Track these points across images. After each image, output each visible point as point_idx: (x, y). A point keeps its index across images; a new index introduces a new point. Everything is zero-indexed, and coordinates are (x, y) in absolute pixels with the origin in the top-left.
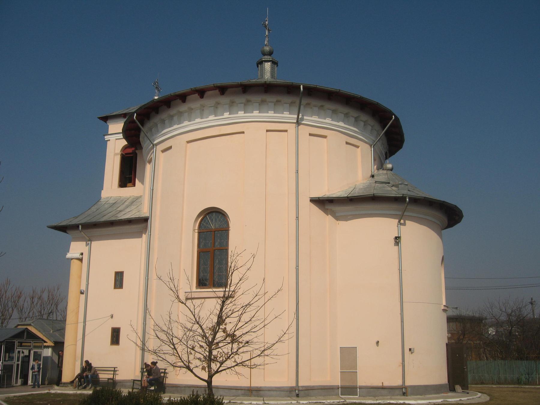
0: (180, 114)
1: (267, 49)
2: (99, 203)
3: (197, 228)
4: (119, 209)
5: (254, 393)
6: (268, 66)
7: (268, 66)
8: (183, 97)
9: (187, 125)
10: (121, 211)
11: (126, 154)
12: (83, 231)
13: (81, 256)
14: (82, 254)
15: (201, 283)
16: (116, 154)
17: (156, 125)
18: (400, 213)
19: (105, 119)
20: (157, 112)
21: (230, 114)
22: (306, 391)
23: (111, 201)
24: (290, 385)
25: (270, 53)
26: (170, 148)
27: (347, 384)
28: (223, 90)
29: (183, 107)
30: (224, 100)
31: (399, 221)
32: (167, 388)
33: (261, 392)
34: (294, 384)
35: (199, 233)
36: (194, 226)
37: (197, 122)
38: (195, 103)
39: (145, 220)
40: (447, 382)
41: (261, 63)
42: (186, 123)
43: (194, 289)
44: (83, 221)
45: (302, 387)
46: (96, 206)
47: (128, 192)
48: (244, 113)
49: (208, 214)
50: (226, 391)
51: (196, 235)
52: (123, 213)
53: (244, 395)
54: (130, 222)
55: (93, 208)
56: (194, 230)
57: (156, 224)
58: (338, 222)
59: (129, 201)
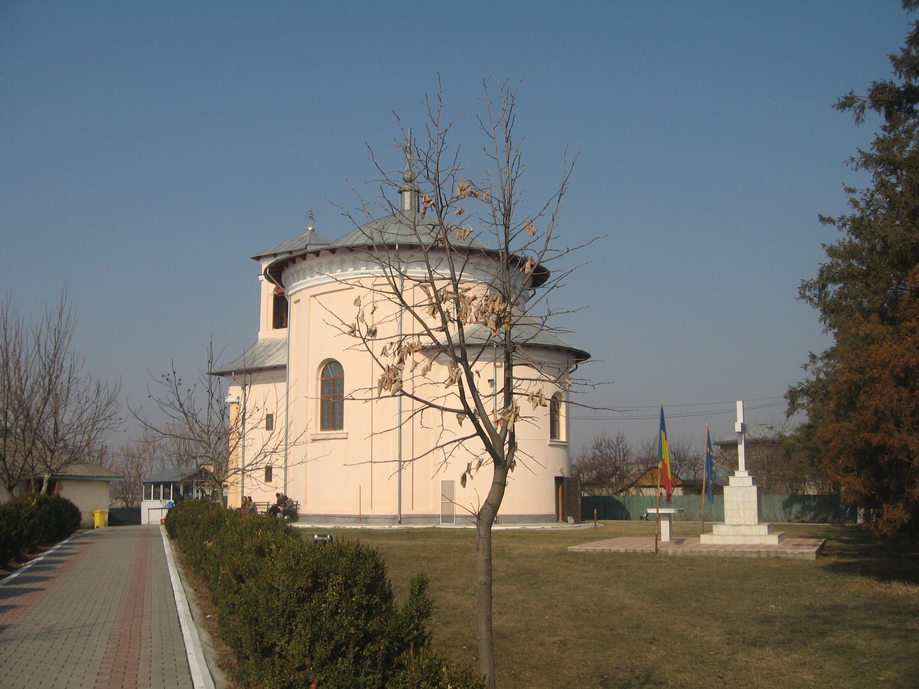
0: (304, 270)
1: (407, 176)
2: (256, 345)
3: (320, 376)
4: (270, 353)
5: (363, 520)
6: (407, 195)
7: (407, 195)
8: (304, 257)
9: (309, 281)
10: (270, 356)
11: (279, 294)
12: (236, 376)
13: (238, 400)
14: (238, 398)
15: (324, 426)
16: (269, 295)
17: (293, 275)
18: (492, 356)
19: (258, 258)
20: (287, 266)
21: (342, 271)
22: (408, 519)
23: (266, 344)
24: (393, 514)
25: (411, 181)
26: (298, 301)
27: (447, 513)
28: (333, 251)
29: (304, 264)
30: (336, 258)
31: (495, 365)
32: (300, 518)
33: (369, 520)
34: (396, 513)
35: (322, 381)
36: (317, 375)
37: (317, 279)
38: (312, 261)
39: (283, 367)
40: (554, 513)
41: (401, 192)
42: (308, 279)
43: (319, 432)
44: (235, 369)
45: (405, 515)
46: (252, 350)
47: (281, 333)
48: (354, 270)
49: (329, 363)
50: (342, 518)
51: (320, 382)
52: (271, 358)
53: (355, 522)
54: (275, 368)
55: (250, 351)
56: (318, 379)
57: (292, 372)
58: (441, 366)
59: (281, 343)
